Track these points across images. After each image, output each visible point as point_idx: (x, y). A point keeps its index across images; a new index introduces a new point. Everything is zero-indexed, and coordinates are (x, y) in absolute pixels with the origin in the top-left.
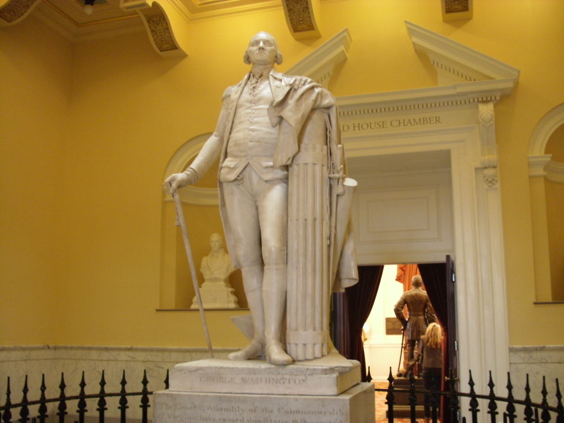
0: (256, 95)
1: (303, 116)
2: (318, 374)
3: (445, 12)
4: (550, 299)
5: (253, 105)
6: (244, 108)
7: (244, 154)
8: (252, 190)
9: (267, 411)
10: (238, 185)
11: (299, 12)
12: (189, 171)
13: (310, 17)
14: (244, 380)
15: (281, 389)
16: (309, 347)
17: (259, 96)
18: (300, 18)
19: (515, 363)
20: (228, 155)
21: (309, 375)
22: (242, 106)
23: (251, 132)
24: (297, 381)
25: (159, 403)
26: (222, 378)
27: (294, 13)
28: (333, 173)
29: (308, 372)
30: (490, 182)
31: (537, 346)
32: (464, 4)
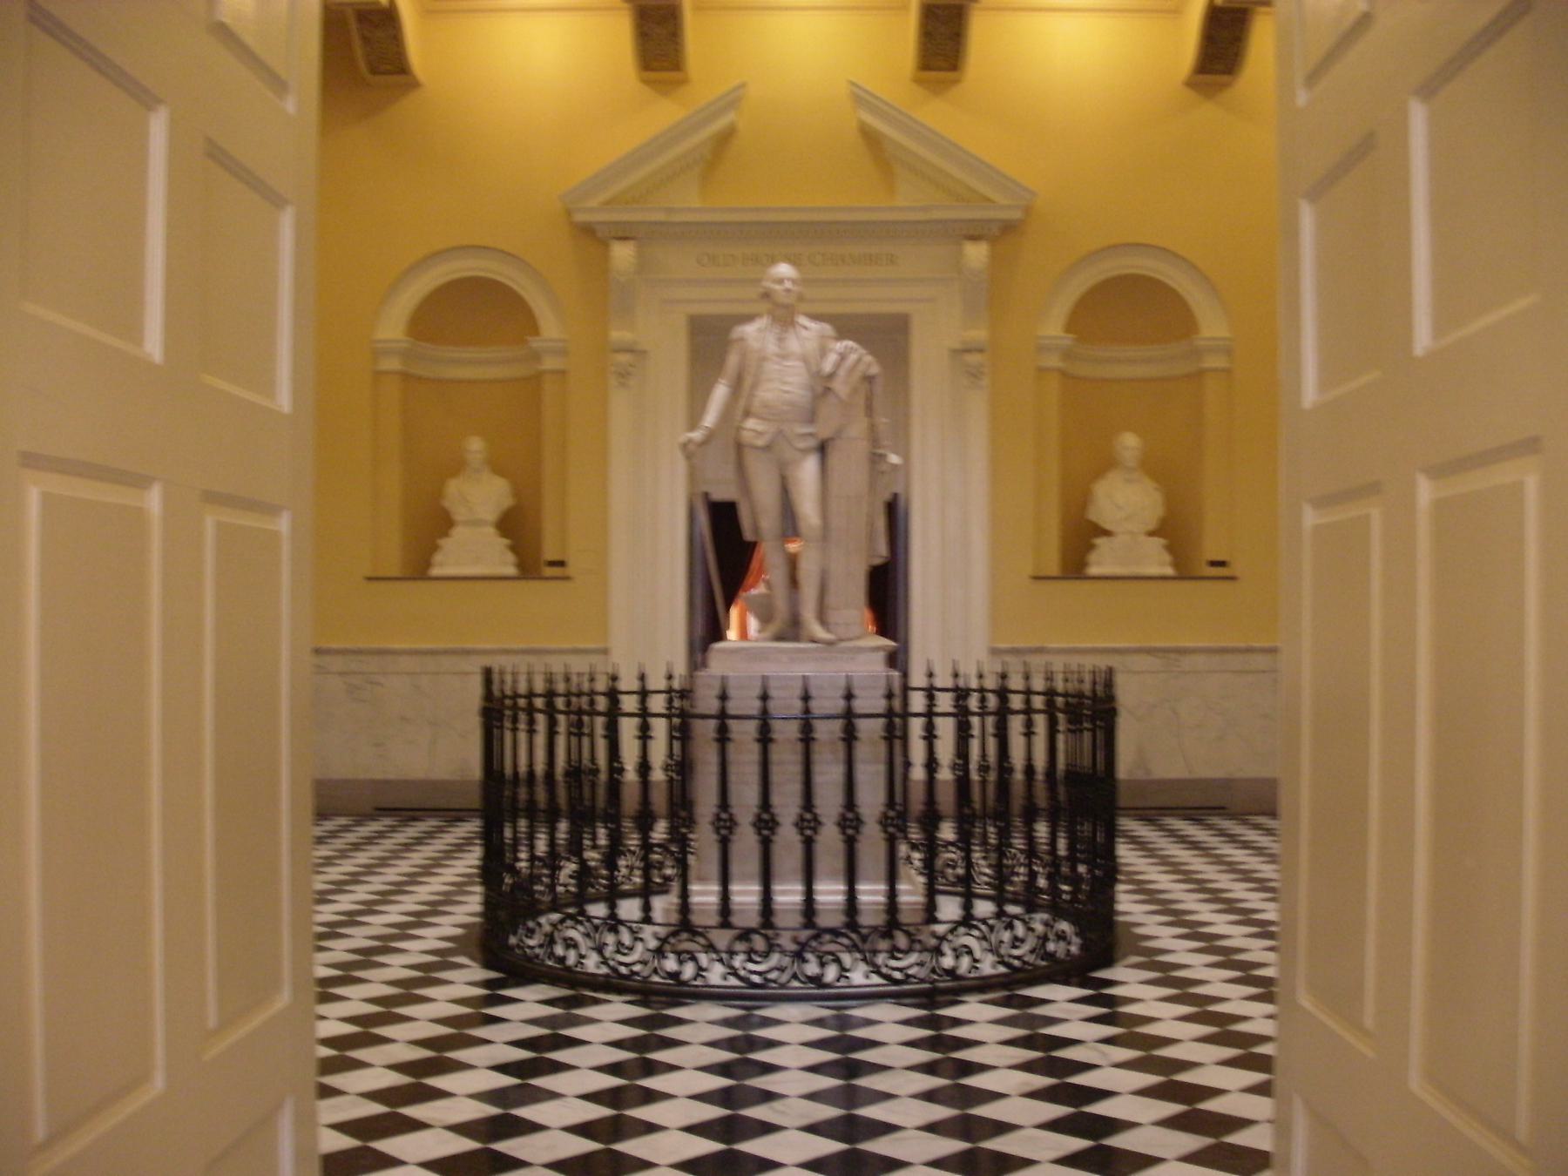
30: (974, 376)
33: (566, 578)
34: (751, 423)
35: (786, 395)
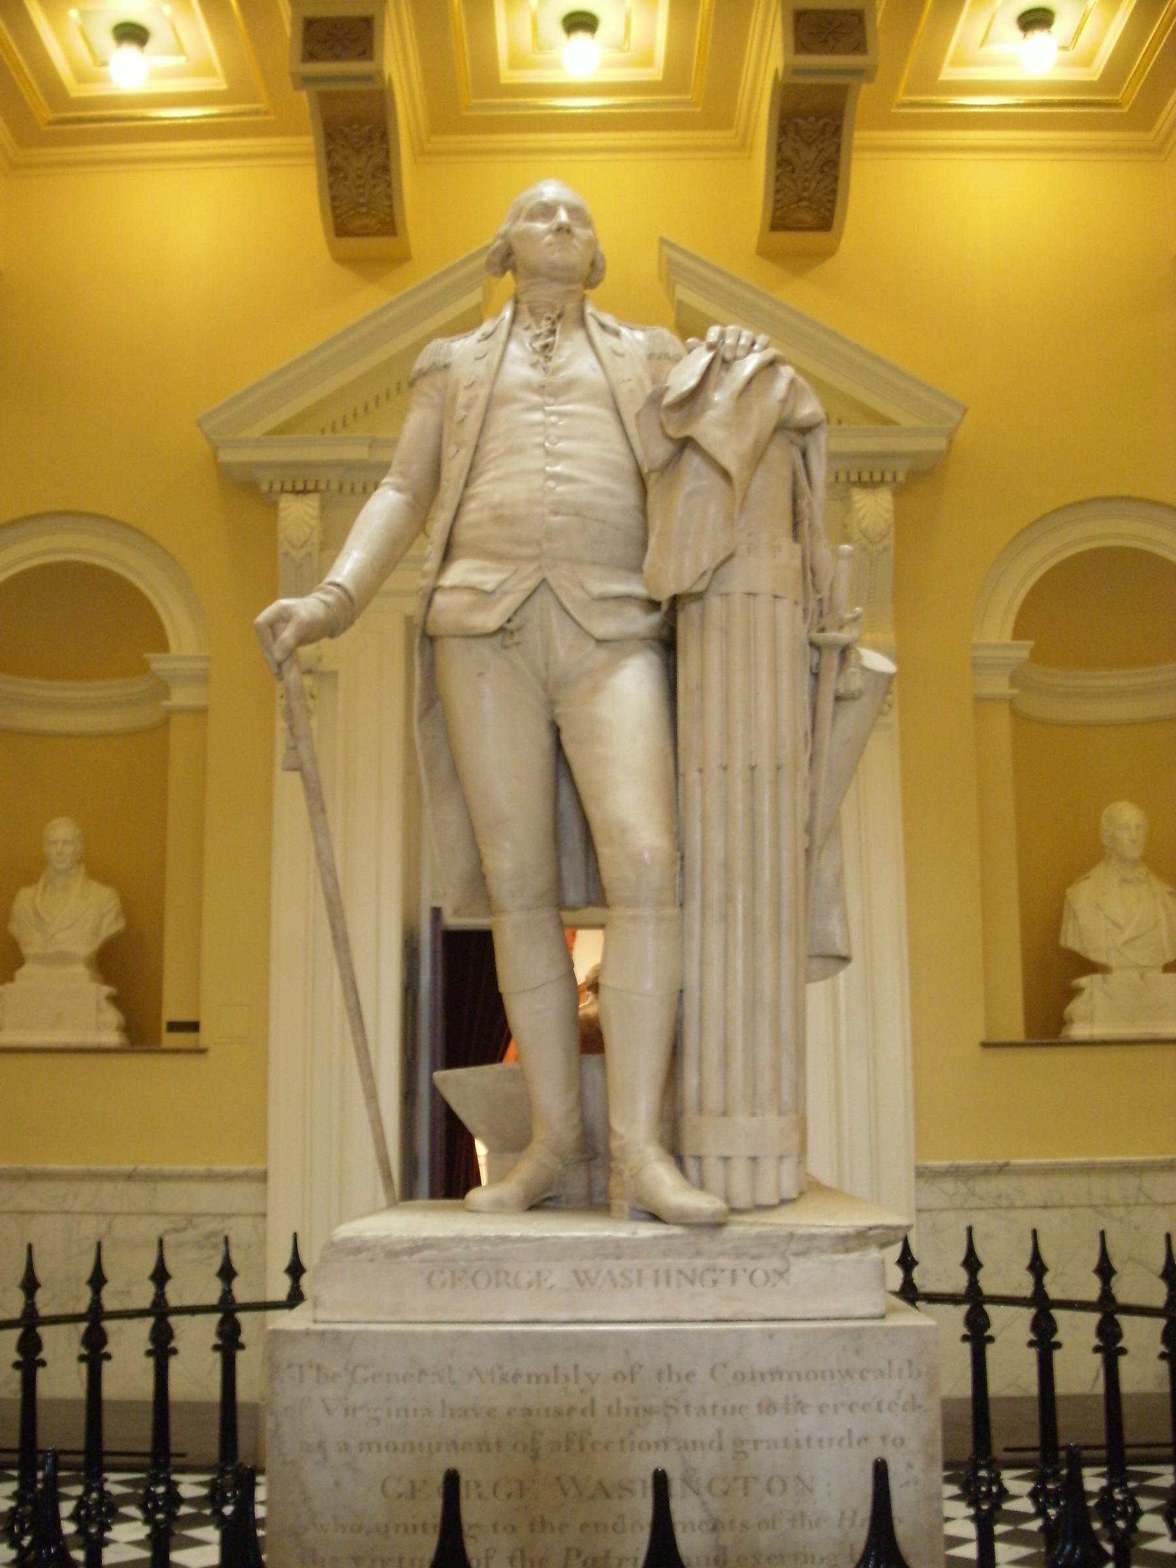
0: (557, 370)
1: (756, 441)
2: (823, 1251)
3: (768, 225)
4: (1019, 1035)
5: (550, 400)
6: (518, 406)
7: (528, 551)
8: (547, 666)
9: (674, 1378)
10: (505, 647)
11: (360, 177)
12: (329, 592)
13: (390, 197)
14: (582, 1276)
15: (709, 1302)
16: (767, 1167)
17: (565, 374)
18: (361, 195)
19: (929, 1210)
20: (456, 552)
21: (796, 1255)
22: (507, 400)
23: (551, 484)
24: (759, 1276)
25: (289, 1366)
26: (507, 1274)
27: (345, 178)
28: (822, 630)
29: (793, 1247)
31: (989, 1162)
32: (822, 210)
33: (202, 1051)
34: (459, 572)
35: (562, 488)
